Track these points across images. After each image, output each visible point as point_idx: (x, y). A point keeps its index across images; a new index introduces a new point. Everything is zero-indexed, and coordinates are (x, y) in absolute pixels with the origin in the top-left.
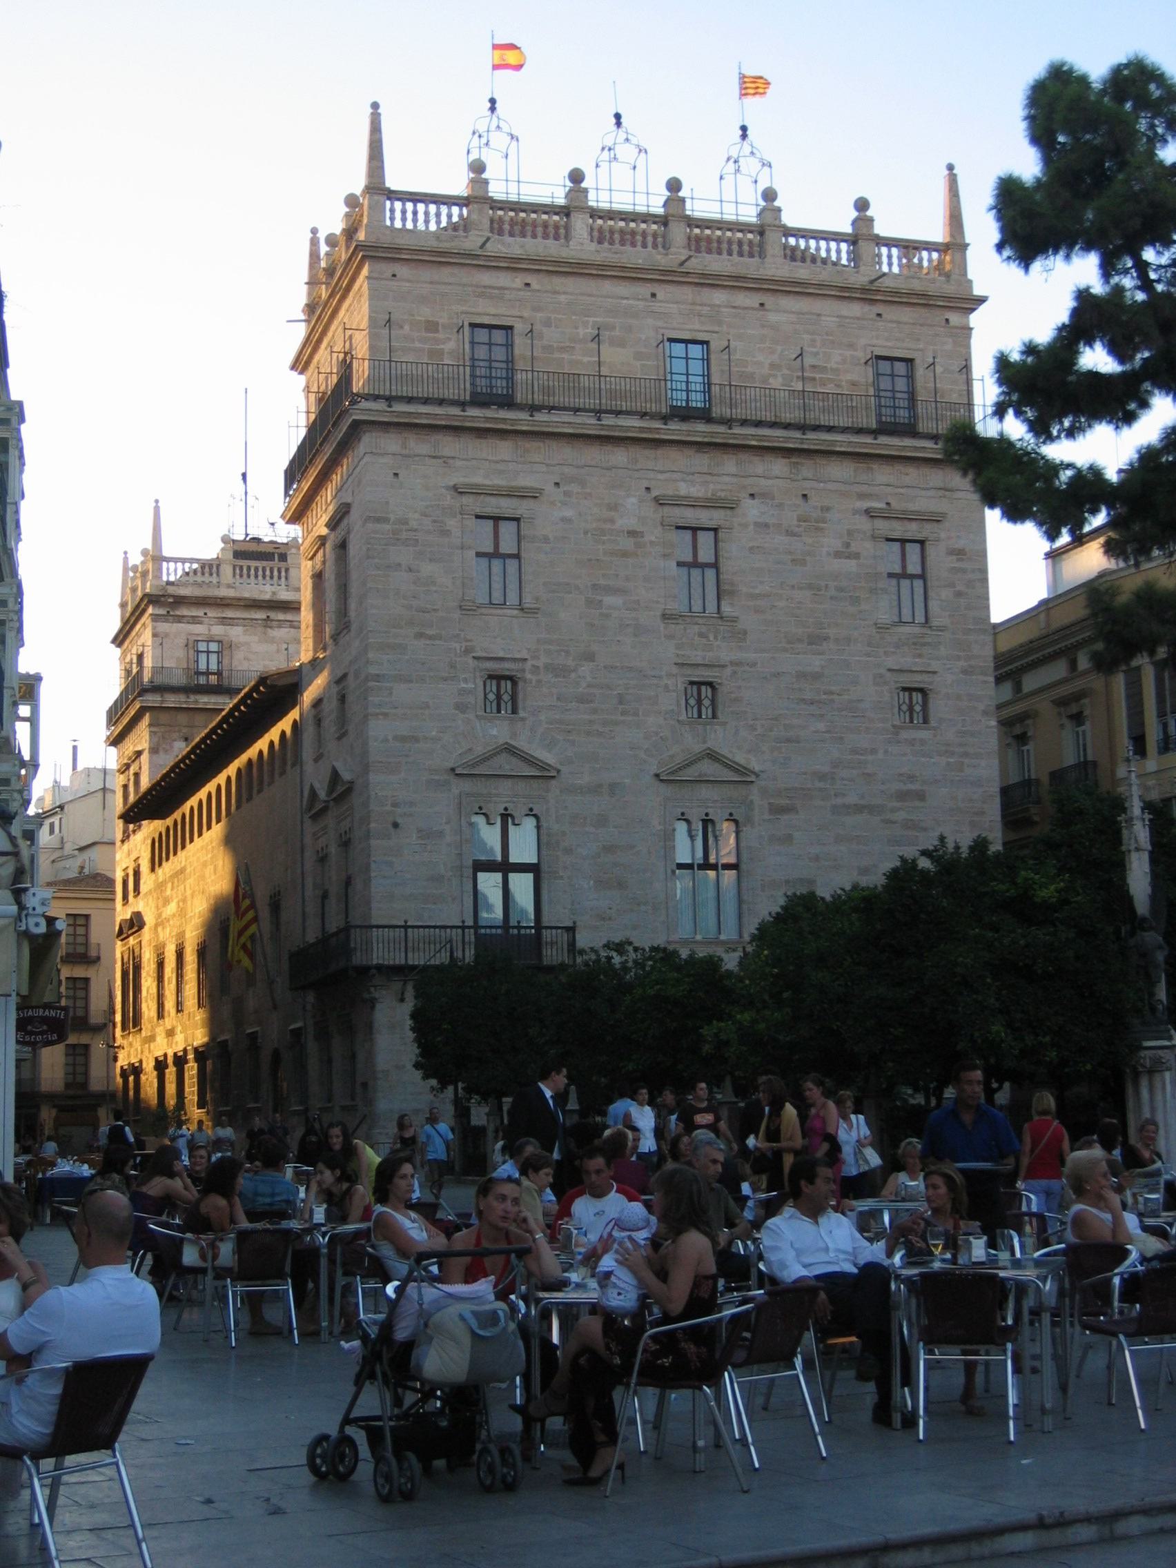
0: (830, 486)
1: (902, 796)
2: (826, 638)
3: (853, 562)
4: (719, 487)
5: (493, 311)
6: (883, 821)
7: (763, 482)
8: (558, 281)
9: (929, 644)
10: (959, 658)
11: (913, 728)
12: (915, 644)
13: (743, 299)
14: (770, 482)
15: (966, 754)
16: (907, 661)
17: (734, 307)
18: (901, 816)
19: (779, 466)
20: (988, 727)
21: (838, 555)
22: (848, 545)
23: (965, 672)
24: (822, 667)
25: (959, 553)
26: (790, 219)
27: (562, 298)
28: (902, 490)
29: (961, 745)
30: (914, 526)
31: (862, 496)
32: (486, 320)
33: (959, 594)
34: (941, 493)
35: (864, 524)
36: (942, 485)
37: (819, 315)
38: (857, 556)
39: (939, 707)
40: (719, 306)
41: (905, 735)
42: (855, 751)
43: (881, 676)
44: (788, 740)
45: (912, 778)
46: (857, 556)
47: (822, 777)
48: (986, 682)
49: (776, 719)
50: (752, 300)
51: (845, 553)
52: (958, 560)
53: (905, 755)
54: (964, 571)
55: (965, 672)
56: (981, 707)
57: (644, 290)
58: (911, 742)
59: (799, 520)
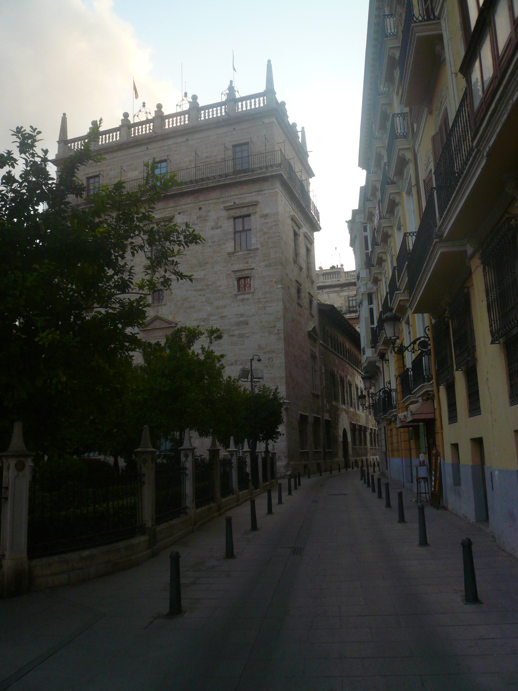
0: (210, 202)
1: (239, 324)
2: (207, 263)
3: (219, 230)
4: (167, 213)
5: (93, 171)
6: (229, 336)
7: (184, 207)
8: (115, 154)
9: (251, 257)
10: (264, 261)
11: (241, 294)
12: (244, 258)
13: (180, 140)
14: (186, 206)
15: (267, 301)
16: (242, 266)
17: (176, 143)
18: (236, 332)
19: (189, 200)
20: (277, 288)
21: (212, 229)
22: (217, 223)
23: (266, 266)
24: (205, 275)
25: (266, 216)
26: (202, 102)
27: (116, 159)
28: (240, 196)
29: (264, 298)
30: (245, 209)
31: (223, 202)
32: (91, 175)
33: (265, 233)
34: (257, 193)
35: (225, 214)
36: (258, 190)
37: (209, 136)
38: (220, 227)
39: (255, 283)
40: (171, 145)
41: (239, 297)
42: (217, 308)
43: (229, 274)
44: (190, 308)
45: (242, 315)
46: (220, 227)
47: (204, 320)
48: (276, 269)
49: (185, 300)
50: (184, 139)
51: (216, 227)
52: (265, 219)
53: (240, 306)
54: (267, 223)
55: (266, 266)
56: (275, 280)
57: (144, 148)
58: (243, 300)
59: (197, 218)
